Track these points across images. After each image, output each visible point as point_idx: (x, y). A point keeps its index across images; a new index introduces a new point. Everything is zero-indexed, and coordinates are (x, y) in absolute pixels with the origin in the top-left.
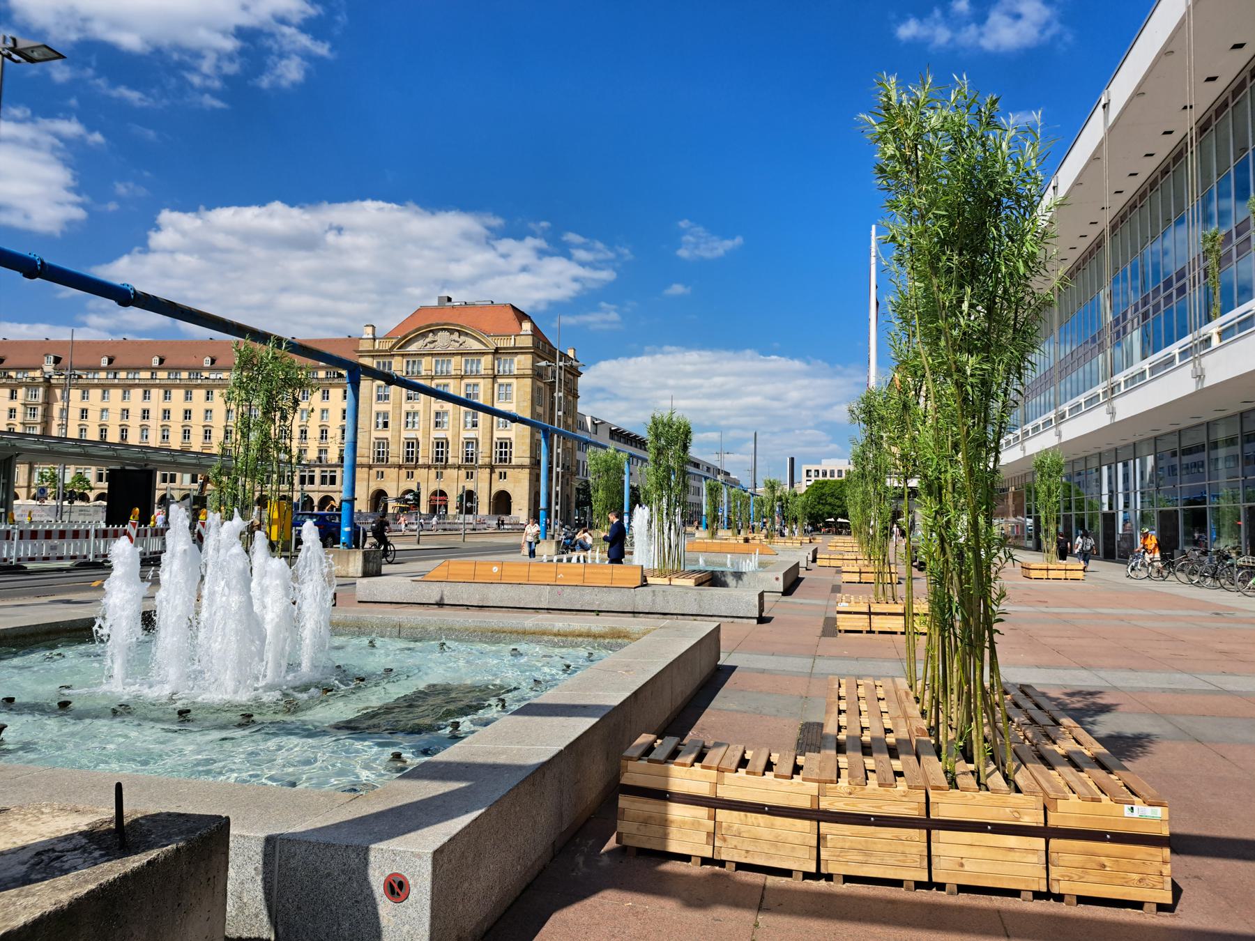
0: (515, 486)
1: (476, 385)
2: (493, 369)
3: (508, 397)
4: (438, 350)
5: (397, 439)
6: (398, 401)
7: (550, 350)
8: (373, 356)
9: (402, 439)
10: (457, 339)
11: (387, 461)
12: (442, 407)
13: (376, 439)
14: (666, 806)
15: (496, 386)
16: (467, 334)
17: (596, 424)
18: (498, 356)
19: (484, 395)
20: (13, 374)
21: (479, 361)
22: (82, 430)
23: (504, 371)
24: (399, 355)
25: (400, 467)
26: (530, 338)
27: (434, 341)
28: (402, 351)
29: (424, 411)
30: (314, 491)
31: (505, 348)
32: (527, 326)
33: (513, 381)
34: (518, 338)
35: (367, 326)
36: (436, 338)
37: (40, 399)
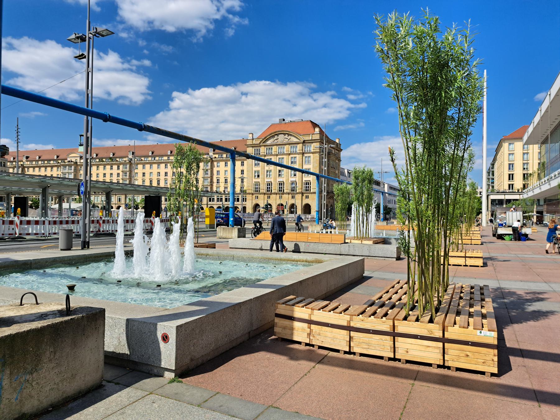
0: (312, 202)
1: (295, 157)
2: (303, 150)
3: (309, 162)
4: (279, 143)
5: (263, 182)
6: (263, 166)
7: (328, 140)
9: (265, 182)
10: (287, 137)
11: (259, 192)
12: (269, 168)
13: (255, 182)
14: (293, 322)
15: (304, 157)
16: (291, 135)
17: (350, 173)
18: (305, 144)
19: (299, 162)
20: (118, 159)
22: (143, 181)
23: (307, 151)
24: (263, 146)
25: (265, 194)
26: (319, 135)
27: (278, 139)
29: (274, 170)
30: (214, 205)
31: (308, 140)
32: (317, 130)
33: (311, 155)
34: (313, 135)
35: (250, 134)
36: (278, 138)
37: (128, 169)
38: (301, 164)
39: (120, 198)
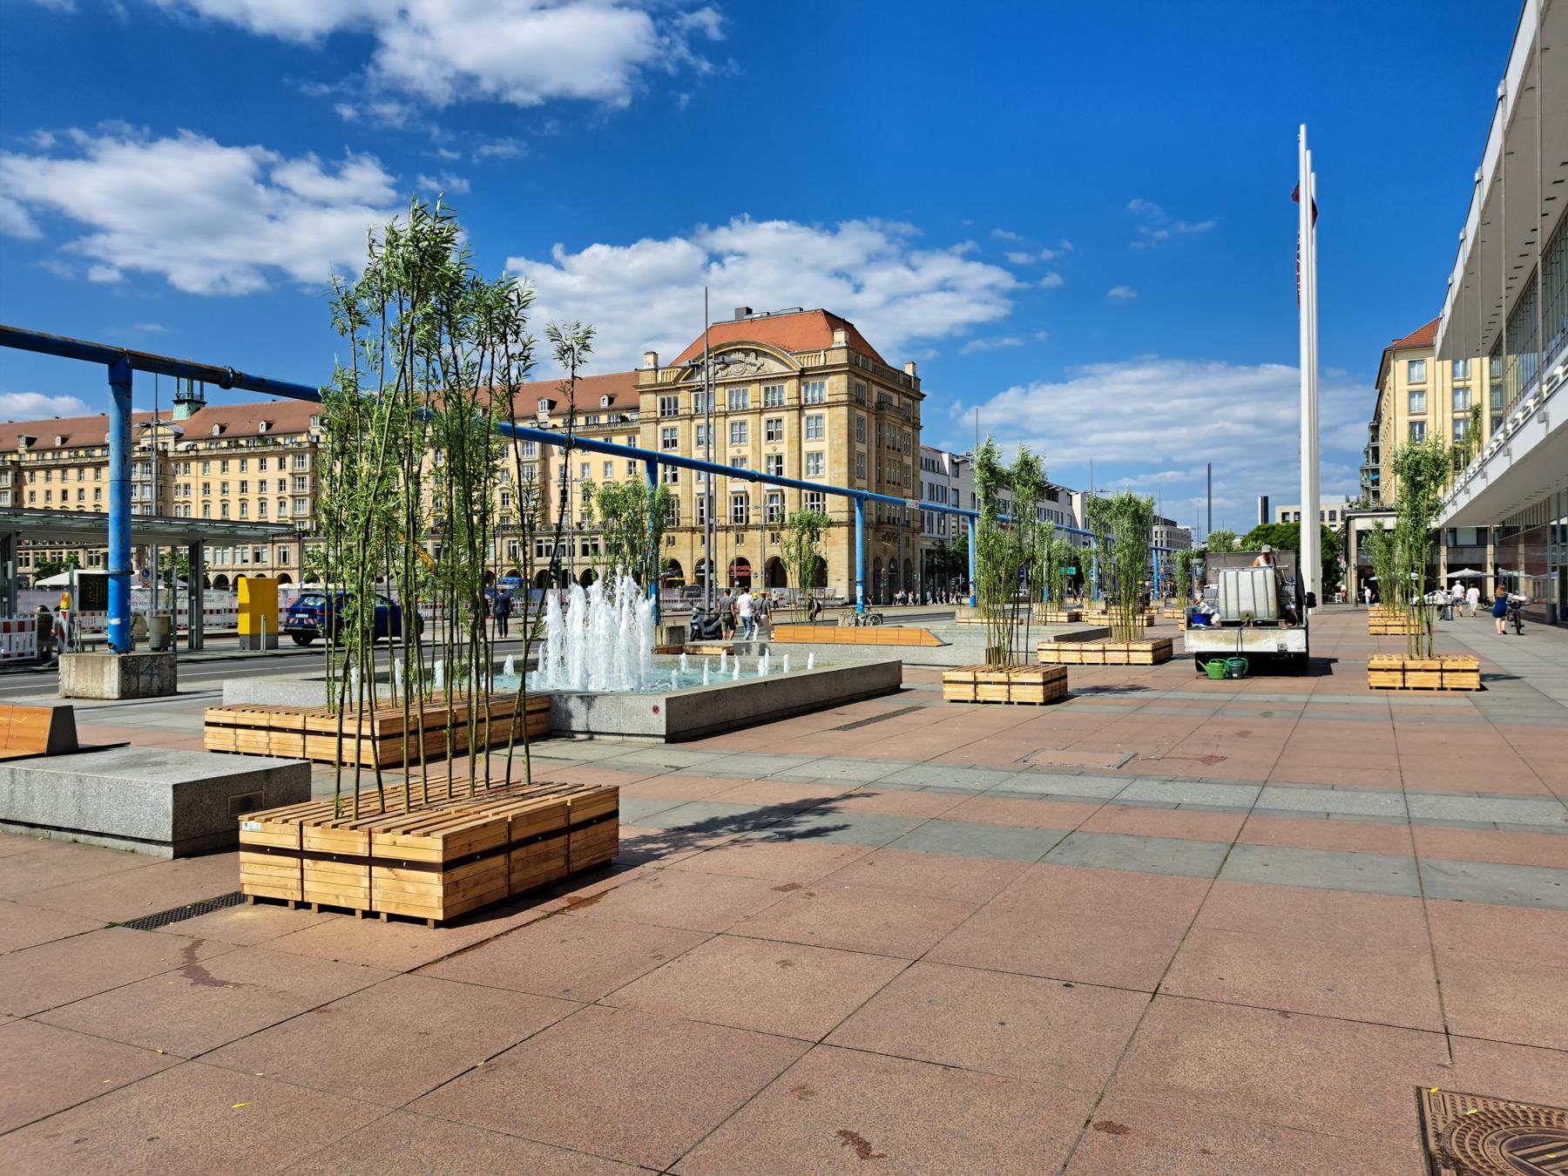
1: (778, 421)
2: (799, 398)
3: (818, 433)
5: (688, 495)
6: (687, 447)
7: (875, 367)
8: (655, 392)
9: (694, 495)
10: (754, 361)
11: (678, 524)
15: (804, 419)
16: (765, 354)
17: (957, 464)
18: (804, 380)
19: (789, 433)
20: (280, 440)
21: (745, 393)
23: (813, 399)
25: (693, 530)
26: (844, 352)
28: (689, 383)
31: (812, 369)
32: (840, 337)
33: (825, 411)
34: (828, 353)
35: (648, 353)
37: (307, 468)
38: (797, 439)
39: (285, 553)
